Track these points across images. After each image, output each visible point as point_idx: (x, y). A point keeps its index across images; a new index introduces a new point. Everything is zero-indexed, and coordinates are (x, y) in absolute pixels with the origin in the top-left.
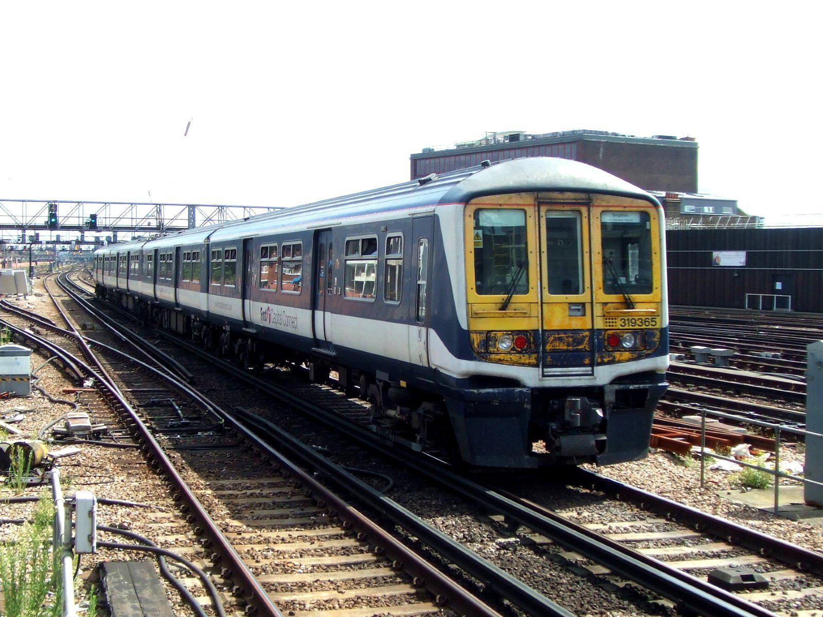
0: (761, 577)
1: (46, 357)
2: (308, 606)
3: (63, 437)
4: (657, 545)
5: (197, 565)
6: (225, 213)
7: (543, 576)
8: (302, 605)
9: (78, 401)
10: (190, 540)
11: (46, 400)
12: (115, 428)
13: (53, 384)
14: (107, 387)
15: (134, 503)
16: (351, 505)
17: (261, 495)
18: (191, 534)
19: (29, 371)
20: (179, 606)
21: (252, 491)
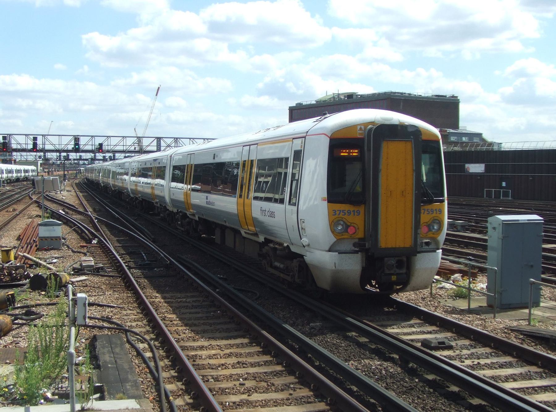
0: (450, 344)
1: (71, 227)
2: (204, 357)
3: (78, 271)
4: (399, 327)
5: (147, 337)
7: (332, 343)
8: (201, 357)
9: (88, 252)
10: (144, 324)
11: (70, 251)
12: (108, 266)
13: (75, 242)
14: (105, 244)
15: (116, 306)
16: (264, 329)
17: (186, 302)
18: (145, 322)
19: (60, 235)
20: (135, 357)
21: (181, 300)
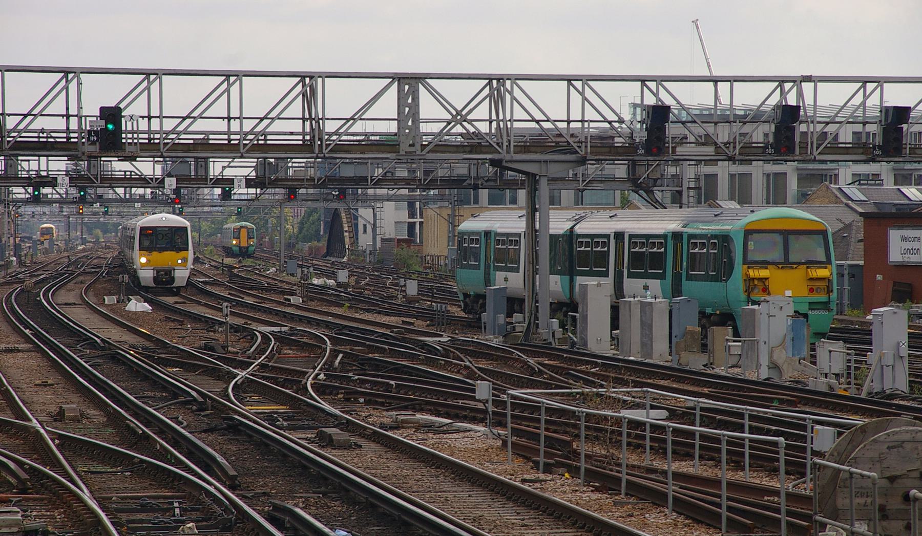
6: (508, 97)
